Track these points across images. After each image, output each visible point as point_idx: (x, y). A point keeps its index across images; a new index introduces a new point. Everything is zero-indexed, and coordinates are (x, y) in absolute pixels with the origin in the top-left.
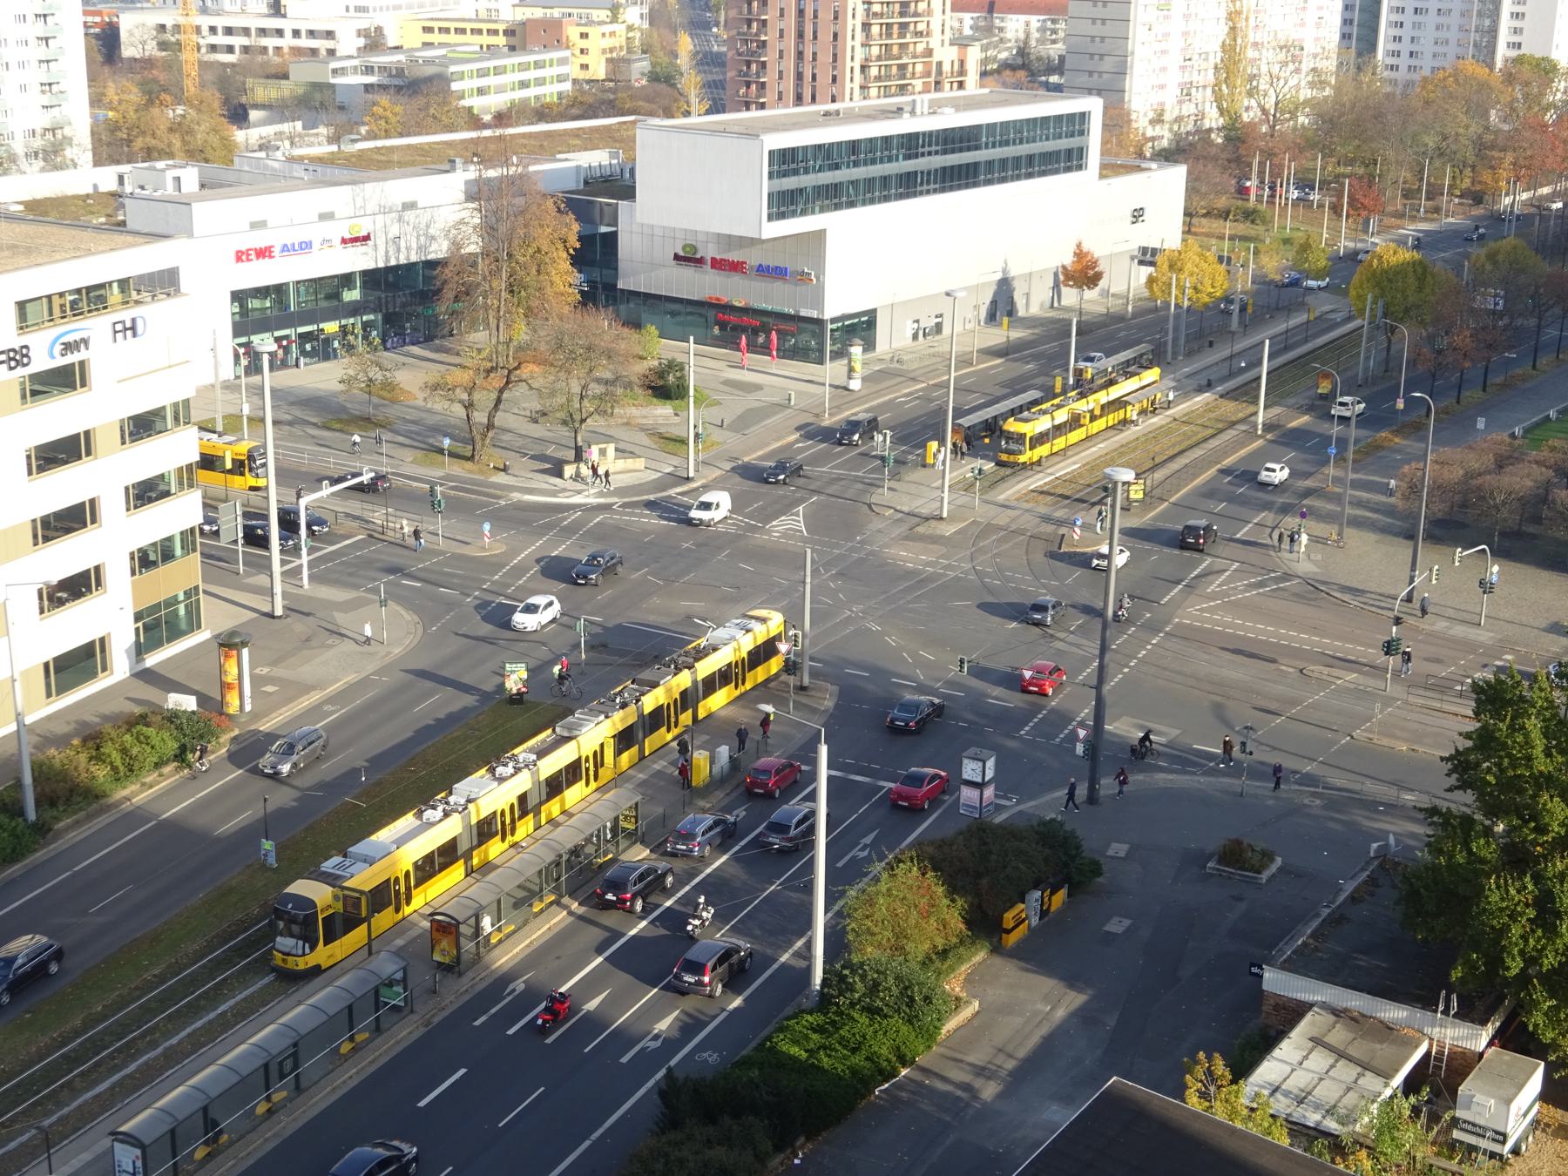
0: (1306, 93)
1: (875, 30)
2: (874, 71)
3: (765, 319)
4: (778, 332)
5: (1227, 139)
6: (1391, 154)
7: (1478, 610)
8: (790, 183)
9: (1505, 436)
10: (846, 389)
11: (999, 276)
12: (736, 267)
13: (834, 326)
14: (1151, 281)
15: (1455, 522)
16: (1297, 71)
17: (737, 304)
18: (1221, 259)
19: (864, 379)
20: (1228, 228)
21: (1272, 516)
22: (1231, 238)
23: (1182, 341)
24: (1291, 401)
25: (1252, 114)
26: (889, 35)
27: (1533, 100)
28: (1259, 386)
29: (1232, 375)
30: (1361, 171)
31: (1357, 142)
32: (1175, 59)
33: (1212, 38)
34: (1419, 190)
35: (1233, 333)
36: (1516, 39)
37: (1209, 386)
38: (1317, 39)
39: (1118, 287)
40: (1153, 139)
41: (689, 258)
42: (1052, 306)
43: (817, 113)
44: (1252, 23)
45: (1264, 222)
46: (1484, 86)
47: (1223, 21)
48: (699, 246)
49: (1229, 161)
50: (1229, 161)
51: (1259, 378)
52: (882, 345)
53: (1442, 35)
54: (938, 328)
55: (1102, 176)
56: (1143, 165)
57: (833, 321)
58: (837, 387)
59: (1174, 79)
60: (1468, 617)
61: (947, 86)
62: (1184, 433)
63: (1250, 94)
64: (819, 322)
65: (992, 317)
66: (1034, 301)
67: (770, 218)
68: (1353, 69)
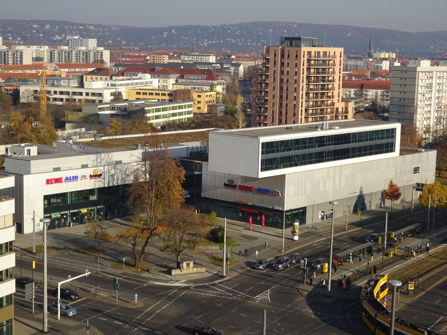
1: (311, 95)
2: (310, 111)
4: (265, 215)
8: (270, 156)
10: (292, 239)
11: (358, 194)
12: (249, 189)
13: (288, 214)
14: (421, 197)
17: (249, 204)
19: (300, 236)
32: (433, 108)
39: (408, 199)
40: (425, 139)
41: (230, 185)
42: (381, 207)
43: (283, 128)
48: (234, 180)
52: (309, 221)
55: (401, 154)
56: (419, 150)
58: (288, 239)
59: (434, 115)
61: (340, 118)
62: (433, 261)
64: (282, 212)
66: (373, 204)
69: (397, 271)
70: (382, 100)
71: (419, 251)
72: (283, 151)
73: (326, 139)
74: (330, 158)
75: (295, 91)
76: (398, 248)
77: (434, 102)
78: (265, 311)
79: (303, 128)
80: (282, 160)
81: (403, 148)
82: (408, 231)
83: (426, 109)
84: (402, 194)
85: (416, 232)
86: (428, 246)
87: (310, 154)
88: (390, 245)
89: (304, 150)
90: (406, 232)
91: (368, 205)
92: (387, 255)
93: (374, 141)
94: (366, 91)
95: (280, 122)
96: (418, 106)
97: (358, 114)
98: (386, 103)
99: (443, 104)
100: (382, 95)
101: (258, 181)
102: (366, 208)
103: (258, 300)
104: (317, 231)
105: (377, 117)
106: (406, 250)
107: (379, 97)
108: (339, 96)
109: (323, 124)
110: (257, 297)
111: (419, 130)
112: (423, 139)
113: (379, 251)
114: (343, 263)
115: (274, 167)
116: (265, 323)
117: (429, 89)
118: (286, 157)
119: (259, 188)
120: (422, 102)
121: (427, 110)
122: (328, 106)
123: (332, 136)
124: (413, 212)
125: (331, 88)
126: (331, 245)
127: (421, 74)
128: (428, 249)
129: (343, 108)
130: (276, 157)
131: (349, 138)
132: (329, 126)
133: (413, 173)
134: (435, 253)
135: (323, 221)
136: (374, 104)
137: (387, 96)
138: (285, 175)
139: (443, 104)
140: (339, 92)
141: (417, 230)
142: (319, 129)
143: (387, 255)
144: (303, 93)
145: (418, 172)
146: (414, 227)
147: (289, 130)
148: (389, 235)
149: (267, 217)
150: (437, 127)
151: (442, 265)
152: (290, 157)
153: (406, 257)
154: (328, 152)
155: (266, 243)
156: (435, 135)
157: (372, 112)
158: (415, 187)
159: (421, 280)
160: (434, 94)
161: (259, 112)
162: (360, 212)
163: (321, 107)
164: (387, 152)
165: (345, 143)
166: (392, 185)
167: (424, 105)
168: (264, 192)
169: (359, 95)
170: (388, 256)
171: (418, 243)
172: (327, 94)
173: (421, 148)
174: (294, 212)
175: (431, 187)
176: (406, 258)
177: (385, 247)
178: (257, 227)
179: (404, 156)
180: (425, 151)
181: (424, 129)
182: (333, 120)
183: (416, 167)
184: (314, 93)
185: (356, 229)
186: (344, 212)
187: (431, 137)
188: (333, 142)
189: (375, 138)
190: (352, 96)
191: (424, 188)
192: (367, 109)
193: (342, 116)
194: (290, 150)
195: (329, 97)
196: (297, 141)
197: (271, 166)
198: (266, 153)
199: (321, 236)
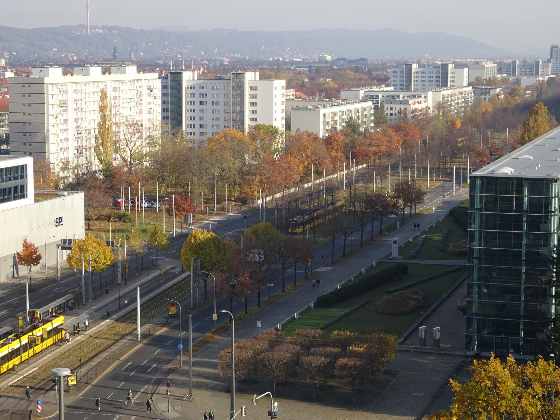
0: (146, 149)
5: (106, 176)
6: (195, 180)
14: (69, 258)
16: (140, 137)
18: (108, 243)
20: (111, 226)
21: (151, 387)
22: (113, 231)
23: (91, 291)
24: (155, 320)
25: (118, 162)
27: (266, 148)
29: (120, 308)
30: (180, 190)
31: (176, 174)
32: (71, 134)
35: (119, 284)
36: (254, 116)
37: (108, 316)
38: (149, 120)
39: (51, 263)
45: (130, 221)
46: (240, 142)
47: (96, 112)
51: (136, 308)
53: (216, 115)
55: (36, 201)
56: (59, 193)
59: (72, 144)
63: (116, 151)
68: (170, 136)
69: (50, 362)
77: (72, 125)
81: (38, 192)
82: (58, 306)
83: (61, 137)
85: (68, 307)
86: (87, 324)
90: (55, 308)
96: (50, 132)
117: (62, 109)
120: (55, 126)
121: (63, 138)
127: (50, 87)
133: (54, 226)
134: (98, 333)
139: (84, 128)
141: (69, 304)
145: (61, 223)
150: (78, 161)
160: (71, 115)
164: (16, 198)
167: (59, 131)
176: (59, 344)
179: (40, 203)
180: (69, 194)
183: (59, 217)
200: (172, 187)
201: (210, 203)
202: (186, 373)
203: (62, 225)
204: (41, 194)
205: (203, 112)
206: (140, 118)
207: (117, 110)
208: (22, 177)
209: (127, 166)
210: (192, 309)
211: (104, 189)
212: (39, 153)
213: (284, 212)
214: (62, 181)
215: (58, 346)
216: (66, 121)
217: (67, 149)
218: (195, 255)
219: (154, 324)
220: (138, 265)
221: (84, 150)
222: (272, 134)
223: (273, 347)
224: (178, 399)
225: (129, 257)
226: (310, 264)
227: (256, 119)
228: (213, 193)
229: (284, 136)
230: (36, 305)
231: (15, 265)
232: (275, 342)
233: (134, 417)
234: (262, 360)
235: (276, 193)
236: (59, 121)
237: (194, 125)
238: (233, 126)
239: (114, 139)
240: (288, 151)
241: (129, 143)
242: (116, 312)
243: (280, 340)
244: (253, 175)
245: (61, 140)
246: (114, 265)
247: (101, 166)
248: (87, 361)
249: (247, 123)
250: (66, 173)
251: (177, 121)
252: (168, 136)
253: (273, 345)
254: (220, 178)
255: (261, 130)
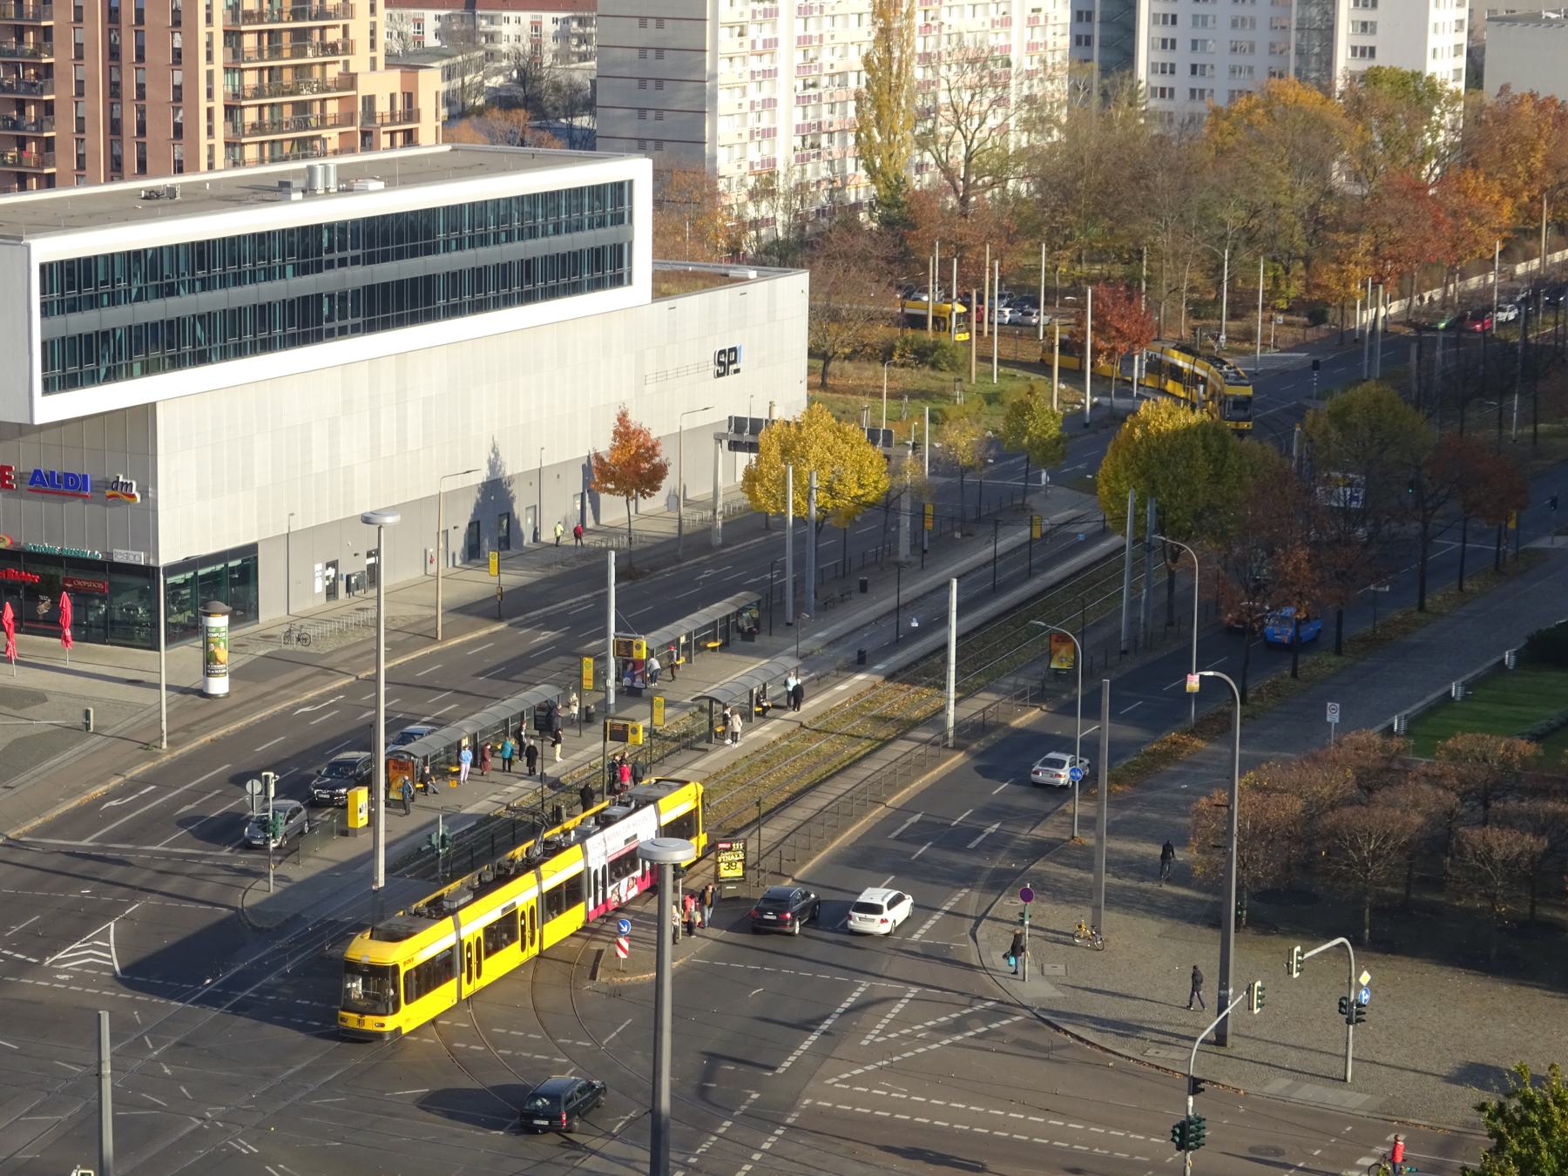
0: (1018, 139)
1: (249, 42)
2: (250, 116)
3: (52, 571)
4: (76, 593)
5: (887, 222)
6: (1164, 241)
7: (1342, 1051)
9: (1373, 735)
10: (202, 693)
11: (481, 476)
13: (178, 579)
14: (751, 477)
15: (1298, 893)
16: (1000, 101)
18: (873, 436)
19: (234, 675)
20: (885, 377)
21: (975, 895)
22: (895, 395)
23: (811, 584)
24: (1008, 682)
25: (927, 178)
26: (276, 52)
27: (1402, 145)
28: (945, 661)
29: (898, 643)
30: (1119, 270)
31: (1106, 223)
32: (785, 87)
33: (849, 41)
34: (1217, 301)
35: (899, 565)
36: (1365, 41)
37: (861, 662)
38: (1032, 47)
40: (756, 224)
44: (919, 19)
45: (954, 365)
46: (1314, 122)
47: (867, 19)
49: (889, 261)
50: (889, 261)
51: (945, 647)
52: (272, 608)
53: (1243, 35)
54: (373, 573)
55: (658, 294)
56: (733, 273)
57: (172, 569)
59: (788, 118)
60: (1321, 1064)
61: (385, 140)
63: (923, 143)
64: (149, 572)
65: (473, 551)
66: (550, 517)
67: (48, 388)
68: (1096, 98)
70: (563, 56)
71: (756, 709)
72: (139, 298)
73: (331, 241)
74: (350, 321)
75: (177, 23)
76: (668, 704)
77: (788, 58)
78: (105, 1017)
79: (222, 191)
80: (138, 338)
81: (667, 268)
83: (754, 94)
84: (670, 469)
85: (740, 630)
87: (262, 307)
88: (631, 694)
89: (234, 291)
91: (526, 525)
92: (620, 735)
93: (541, 241)
94: (492, 20)
95: (116, 169)
97: (464, 123)
98: (582, 73)
99: (826, 70)
100: (563, 36)
101: (33, 437)
102: (522, 536)
103: (66, 971)
104: (312, 649)
105: (546, 135)
106: (701, 709)
107: (550, 46)
108: (373, 45)
109: (311, 170)
110: (59, 956)
111: (729, 187)
112: (745, 225)
113: (587, 718)
114: (434, 783)
115: (103, 372)
116: (107, 1070)
118: (155, 325)
119: (37, 472)
120: (737, 61)
121: (758, 98)
122: (328, 90)
123: (355, 222)
124: (723, 546)
125: (336, 8)
126: (377, 708)
128: (797, 697)
129: (392, 96)
130: (107, 326)
131: (429, 234)
132: (340, 180)
133: (711, 373)
135: (333, 604)
136: (527, 75)
137: (584, 39)
138: (154, 405)
139: (826, 70)
140: (374, 24)
141: (743, 623)
142: (297, 196)
143: (620, 735)
144: (210, 35)
145: (733, 367)
146: (733, 609)
147: (158, 203)
148: (625, 649)
149: (83, 599)
150: (803, 171)
151: (856, 762)
152: (170, 323)
153: (700, 739)
154: (343, 297)
155: (87, 712)
156: (796, 204)
157: (521, 113)
158: (725, 436)
159: (771, 832)
160: (787, 27)
161: (16, 125)
162: (493, 557)
163: (298, 94)
164: (598, 285)
165: (414, 253)
166: (625, 433)
167: (747, 77)
168: (65, 485)
169: (461, 38)
170: (625, 740)
171: (750, 675)
172: (322, 37)
173: (739, 262)
174: (201, 572)
175: (793, 430)
177: (612, 700)
178: (41, 647)
179: (671, 303)
180: (761, 277)
181: (751, 181)
182: (353, 151)
183: (727, 347)
184: (260, 32)
185: (483, 632)
186: (428, 560)
187: (781, 217)
188: (359, 252)
189: (545, 227)
190: (431, 41)
191: (763, 436)
192: (502, 101)
193: (392, 133)
194: (171, 291)
195: (333, 49)
196: (201, 252)
197: (87, 367)
198: (61, 312)
199: (329, 671)
200: (1092, 261)
201: (1206, 317)
202: (1086, 860)
203: (737, 371)
204: (678, 272)
205: (1205, 24)
206: (1002, 41)
207: (931, 14)
208: (619, 219)
209: (956, 191)
210: (1125, 652)
211: (872, 260)
212: (679, 142)
213: (1439, 354)
214: (753, 233)
215: (696, 754)
216: (771, 44)
217: (769, 133)
218: (1141, 481)
219: (1007, 693)
220: (964, 504)
221: (824, 140)
222: (1420, 100)
223: (1370, 790)
224: (1057, 941)
225: (941, 480)
226: (1512, 525)
227: (1372, 51)
228: (1221, 282)
229: (1460, 108)
230: (638, 620)
231: (591, 493)
232: (1382, 771)
233: (915, 990)
234: (1333, 832)
235: (1422, 288)
236: (747, 46)
237: (1173, 66)
238: (1298, 72)
239: (919, 103)
240: (1468, 155)
241: (963, 118)
242: (885, 652)
243: (1396, 766)
244: (1348, 231)
245: (752, 104)
246: (887, 505)
247: (874, 190)
248: (784, 805)
249: (1343, 60)
250: (765, 209)
251: (1121, 53)
252: (1086, 100)
253: (1370, 783)
254: (1244, 237)
255: (1386, 87)
